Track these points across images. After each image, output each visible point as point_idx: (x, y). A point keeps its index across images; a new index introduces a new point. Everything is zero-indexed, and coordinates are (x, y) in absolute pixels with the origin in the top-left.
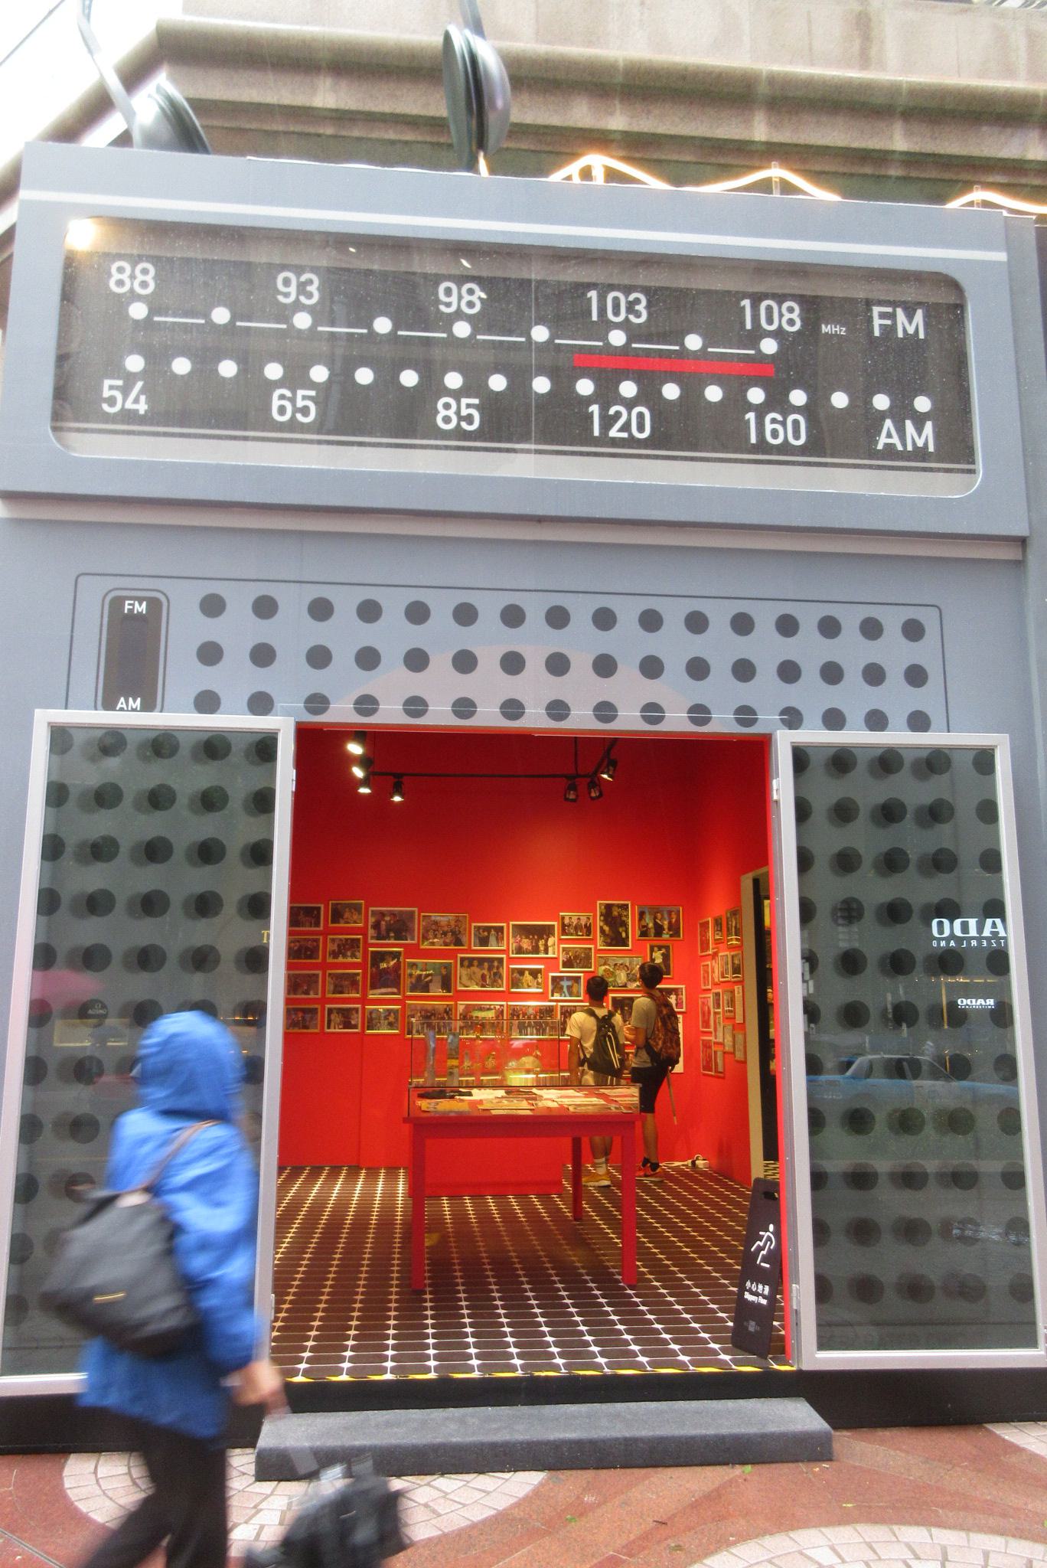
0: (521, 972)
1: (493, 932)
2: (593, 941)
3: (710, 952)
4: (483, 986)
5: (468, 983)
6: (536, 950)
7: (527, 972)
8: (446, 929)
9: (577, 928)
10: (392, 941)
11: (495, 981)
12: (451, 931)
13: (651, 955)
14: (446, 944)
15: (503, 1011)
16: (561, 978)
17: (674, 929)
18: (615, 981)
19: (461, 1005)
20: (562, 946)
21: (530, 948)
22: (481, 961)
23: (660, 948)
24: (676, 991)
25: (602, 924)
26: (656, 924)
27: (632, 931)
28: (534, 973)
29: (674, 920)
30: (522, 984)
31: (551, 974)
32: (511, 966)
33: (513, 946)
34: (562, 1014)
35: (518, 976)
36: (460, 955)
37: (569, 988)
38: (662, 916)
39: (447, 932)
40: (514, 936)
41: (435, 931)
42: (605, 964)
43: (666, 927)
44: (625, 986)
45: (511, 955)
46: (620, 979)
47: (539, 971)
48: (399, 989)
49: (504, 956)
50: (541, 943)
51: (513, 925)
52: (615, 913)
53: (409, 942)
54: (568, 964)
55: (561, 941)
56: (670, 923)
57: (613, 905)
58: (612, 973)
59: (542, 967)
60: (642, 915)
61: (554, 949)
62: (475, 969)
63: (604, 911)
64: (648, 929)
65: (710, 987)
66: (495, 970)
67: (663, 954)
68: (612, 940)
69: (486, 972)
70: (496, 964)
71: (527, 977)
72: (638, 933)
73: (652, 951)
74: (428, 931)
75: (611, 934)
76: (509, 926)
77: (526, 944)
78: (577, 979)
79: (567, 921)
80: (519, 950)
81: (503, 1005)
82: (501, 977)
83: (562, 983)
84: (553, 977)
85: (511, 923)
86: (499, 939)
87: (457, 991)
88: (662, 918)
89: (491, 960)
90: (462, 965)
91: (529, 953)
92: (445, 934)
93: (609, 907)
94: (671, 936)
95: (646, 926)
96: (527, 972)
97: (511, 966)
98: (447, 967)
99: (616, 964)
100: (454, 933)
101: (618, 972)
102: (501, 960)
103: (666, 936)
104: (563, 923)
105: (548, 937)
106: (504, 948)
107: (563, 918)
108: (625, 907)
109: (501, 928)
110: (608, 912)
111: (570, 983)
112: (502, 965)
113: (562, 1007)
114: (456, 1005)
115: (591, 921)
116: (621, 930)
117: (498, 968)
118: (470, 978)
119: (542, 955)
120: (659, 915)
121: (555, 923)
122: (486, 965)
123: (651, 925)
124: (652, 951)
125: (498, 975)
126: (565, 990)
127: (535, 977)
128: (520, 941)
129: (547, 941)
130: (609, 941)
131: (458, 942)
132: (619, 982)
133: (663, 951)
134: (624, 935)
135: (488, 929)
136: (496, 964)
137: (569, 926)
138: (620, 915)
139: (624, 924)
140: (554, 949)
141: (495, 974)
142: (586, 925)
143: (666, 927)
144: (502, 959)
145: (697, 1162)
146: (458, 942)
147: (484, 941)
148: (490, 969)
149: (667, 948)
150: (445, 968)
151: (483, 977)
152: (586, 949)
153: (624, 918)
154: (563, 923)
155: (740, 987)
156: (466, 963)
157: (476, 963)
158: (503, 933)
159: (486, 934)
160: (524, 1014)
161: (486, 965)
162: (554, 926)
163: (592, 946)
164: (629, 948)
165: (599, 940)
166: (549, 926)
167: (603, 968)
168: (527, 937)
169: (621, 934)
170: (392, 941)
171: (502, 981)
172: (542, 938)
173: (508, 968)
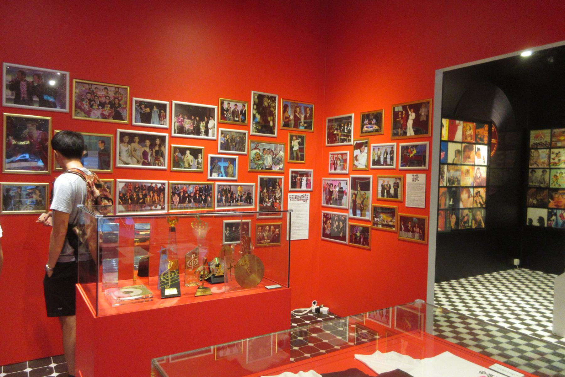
0: (183, 151)
1: (155, 109)
2: (247, 127)
3: (352, 143)
4: (144, 164)
5: (129, 160)
6: (197, 131)
7: (188, 152)
8: (103, 100)
9: (234, 113)
10: (36, 107)
11: (157, 159)
12: (110, 103)
13: (291, 143)
14: (104, 117)
15: (164, 188)
16: (220, 159)
17: (309, 126)
18: (263, 164)
19: (121, 183)
20: (220, 129)
21: (192, 129)
22: (143, 138)
23: (297, 138)
24: (307, 174)
25: (255, 112)
26: (295, 116)
27: (277, 121)
28: (195, 153)
29: (308, 115)
30: (184, 163)
31: (210, 155)
32: (173, 145)
33: (175, 125)
34: (219, 192)
35: (180, 155)
36: (119, 130)
37: (226, 168)
38: (300, 109)
39: (105, 103)
40: (177, 116)
41: (90, 101)
42: (255, 149)
43: (302, 120)
44: (270, 169)
45: (173, 134)
46: (267, 161)
47: (200, 151)
48: (45, 161)
49: (167, 135)
50: (202, 124)
51: (176, 104)
52: (266, 104)
53: (58, 109)
54: (226, 146)
55: (220, 124)
56: (305, 117)
57: (263, 96)
58: (261, 156)
59: (203, 147)
60: (286, 107)
61: (213, 132)
62: (135, 145)
63: (257, 101)
64: (290, 120)
65: (347, 172)
66: (157, 148)
67: (299, 143)
68: (262, 127)
69: (147, 149)
70: (158, 141)
71: (189, 157)
72: (282, 123)
73: (292, 139)
74: (82, 100)
75: (261, 121)
76: (171, 105)
77: (188, 124)
78: (233, 161)
79: (226, 106)
80: (181, 130)
81: (164, 184)
82: (163, 155)
83: (220, 164)
84: (212, 158)
85: (174, 102)
86: (161, 117)
87: (116, 168)
88: (300, 113)
89: (152, 138)
90: (122, 141)
91: (189, 134)
92: (102, 105)
93: (261, 97)
94: (306, 128)
95: (288, 118)
96: (188, 152)
97: (173, 145)
98: (104, 141)
99: (264, 149)
100: (112, 105)
101: (265, 156)
102: (163, 139)
103: (302, 128)
104: (222, 107)
105: (209, 119)
106: (167, 126)
107: (222, 103)
108: (273, 99)
109: (163, 107)
110: (259, 104)
111: (226, 164)
112: (165, 142)
113: (219, 186)
114: (115, 182)
115: (246, 108)
116: (269, 119)
117: (160, 146)
118: (131, 155)
119: (203, 136)
120: (298, 109)
121: (216, 107)
122: (148, 143)
123: (292, 117)
124: (292, 139)
125: (159, 154)
126: (222, 170)
127: (196, 157)
128: (182, 121)
129: (207, 123)
130: (260, 128)
131: (118, 116)
132: (266, 164)
133: (300, 140)
134: (271, 124)
135: (151, 105)
136: (158, 141)
137: (227, 111)
138: (269, 106)
139: (272, 114)
140: (213, 132)
141: (157, 152)
142: (242, 111)
143: (302, 120)
144: (164, 137)
145: (321, 309)
146: (118, 116)
147: (146, 118)
148: (152, 147)
149: (302, 138)
150: (103, 142)
151: (145, 154)
152: (241, 133)
153: (272, 109)
154: (222, 107)
155: (422, 177)
156: (126, 139)
157: (137, 139)
158: (165, 111)
159: (148, 110)
160: (185, 192)
161: (148, 143)
162: (214, 109)
163: (246, 132)
164: (276, 135)
165: (252, 127)
166: (210, 109)
167: (254, 152)
168: (189, 118)
169: (269, 122)
170: (36, 107)
171: (164, 159)
172: (203, 120)
173: (170, 147)
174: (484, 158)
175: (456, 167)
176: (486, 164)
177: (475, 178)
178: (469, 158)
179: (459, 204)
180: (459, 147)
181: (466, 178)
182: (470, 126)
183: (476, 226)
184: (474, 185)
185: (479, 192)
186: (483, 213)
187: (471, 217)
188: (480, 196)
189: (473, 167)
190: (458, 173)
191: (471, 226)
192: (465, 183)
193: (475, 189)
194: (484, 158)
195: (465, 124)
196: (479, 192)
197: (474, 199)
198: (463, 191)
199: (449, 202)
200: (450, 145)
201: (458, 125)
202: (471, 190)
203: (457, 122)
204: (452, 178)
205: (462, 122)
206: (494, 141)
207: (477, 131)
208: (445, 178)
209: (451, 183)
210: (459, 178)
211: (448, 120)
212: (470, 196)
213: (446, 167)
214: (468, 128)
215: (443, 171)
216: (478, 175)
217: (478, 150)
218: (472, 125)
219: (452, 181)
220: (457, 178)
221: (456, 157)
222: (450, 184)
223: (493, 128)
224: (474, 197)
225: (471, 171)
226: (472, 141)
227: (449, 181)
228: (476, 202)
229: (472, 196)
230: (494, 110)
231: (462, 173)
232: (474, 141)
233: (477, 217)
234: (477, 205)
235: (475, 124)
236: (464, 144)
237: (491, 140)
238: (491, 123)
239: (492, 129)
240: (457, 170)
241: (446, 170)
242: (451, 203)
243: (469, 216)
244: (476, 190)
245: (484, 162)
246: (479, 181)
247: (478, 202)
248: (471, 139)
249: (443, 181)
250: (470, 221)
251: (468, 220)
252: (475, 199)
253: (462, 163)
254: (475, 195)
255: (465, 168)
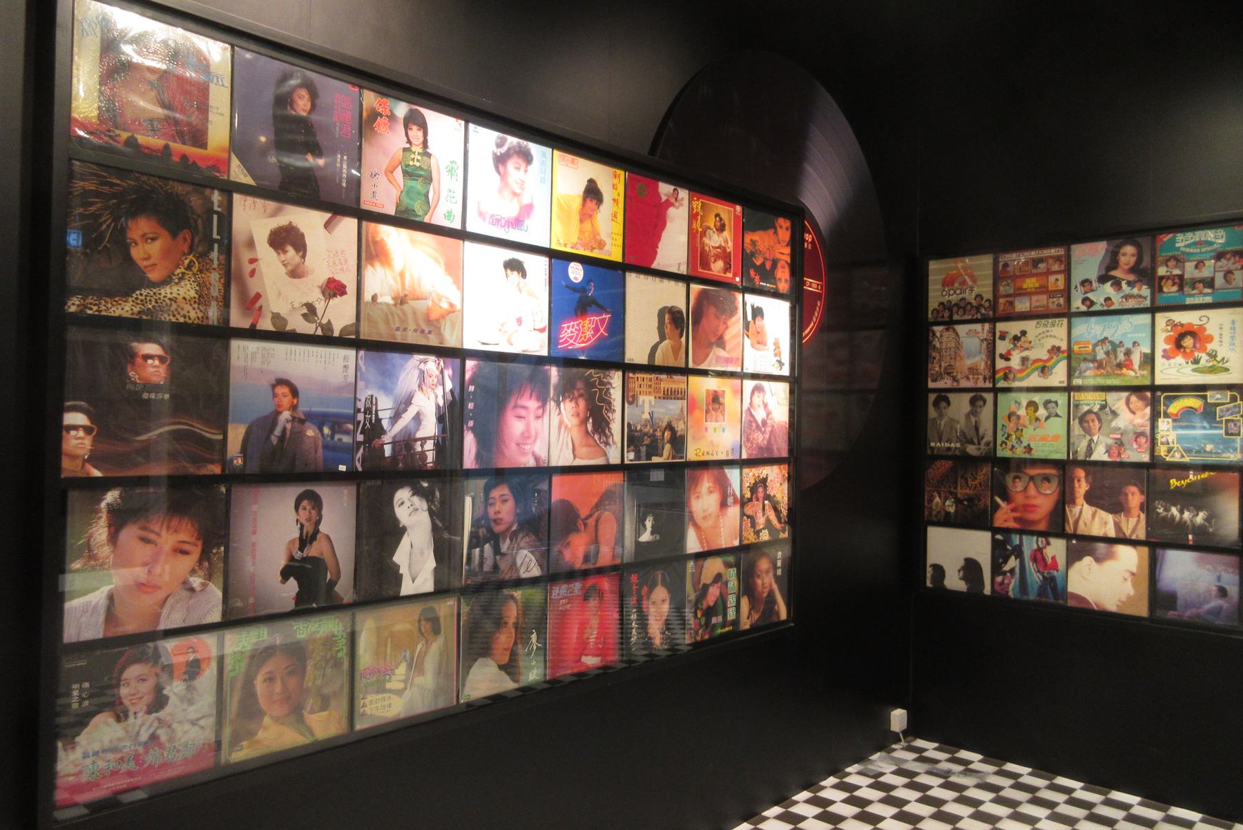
174: (777, 345)
175: (667, 383)
176: (786, 371)
177: (749, 425)
178: (721, 342)
179: (682, 538)
180: (675, 295)
181: (711, 425)
182: (717, 215)
183: (756, 616)
184: (744, 456)
185: (764, 481)
186: (779, 564)
187: (733, 584)
188: (768, 497)
189: (738, 382)
190: (675, 407)
191: (736, 623)
192: (704, 447)
193: (746, 471)
194: (777, 345)
195: (697, 204)
196: (764, 481)
197: (743, 514)
198: (696, 482)
199: (638, 533)
200: (634, 282)
201: (668, 204)
202: (733, 475)
203: (665, 189)
204: (648, 429)
205: (684, 194)
206: (812, 285)
207: (747, 240)
208: (616, 427)
209: (643, 449)
210: (680, 427)
211: (621, 173)
212: (730, 500)
213: (616, 378)
214: (711, 222)
215: (602, 400)
216: (760, 415)
217: (754, 317)
218: (729, 212)
219: (647, 441)
220: (670, 427)
221: (662, 337)
222: (638, 457)
223: (808, 237)
224: (743, 503)
225: (729, 400)
226: (730, 275)
227: (633, 438)
228: (753, 525)
229: (735, 502)
230: (809, 169)
231: (692, 406)
232: (738, 279)
233: (759, 582)
234: (757, 533)
235: (739, 208)
236: (695, 288)
237: (804, 283)
238: (798, 215)
239: (804, 240)
240: (670, 395)
241: (616, 395)
242: (646, 537)
243: (726, 583)
244: (752, 474)
245: (781, 363)
246: (760, 438)
247: (761, 521)
248: (726, 270)
249: (607, 444)
250: (731, 600)
251: (723, 599)
252: (748, 511)
253: (691, 365)
254: (748, 495)
255: (702, 386)
